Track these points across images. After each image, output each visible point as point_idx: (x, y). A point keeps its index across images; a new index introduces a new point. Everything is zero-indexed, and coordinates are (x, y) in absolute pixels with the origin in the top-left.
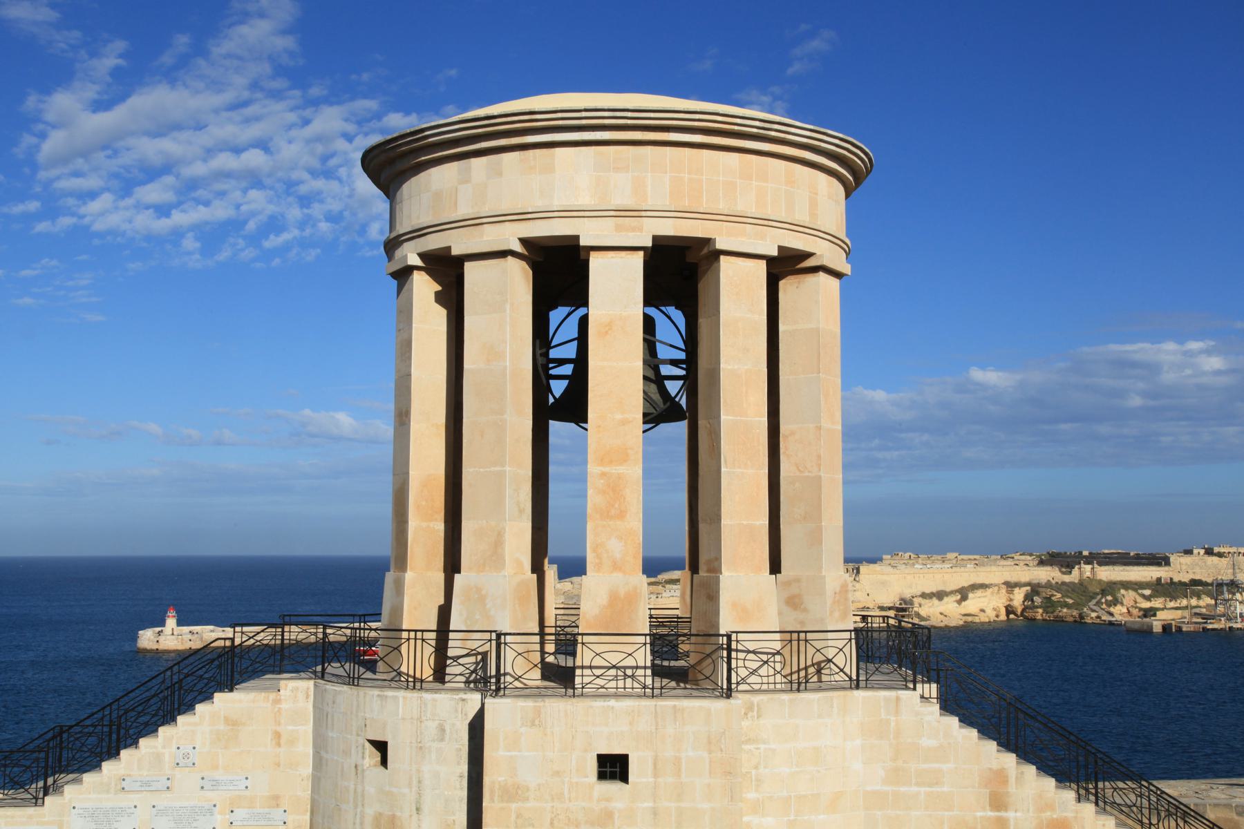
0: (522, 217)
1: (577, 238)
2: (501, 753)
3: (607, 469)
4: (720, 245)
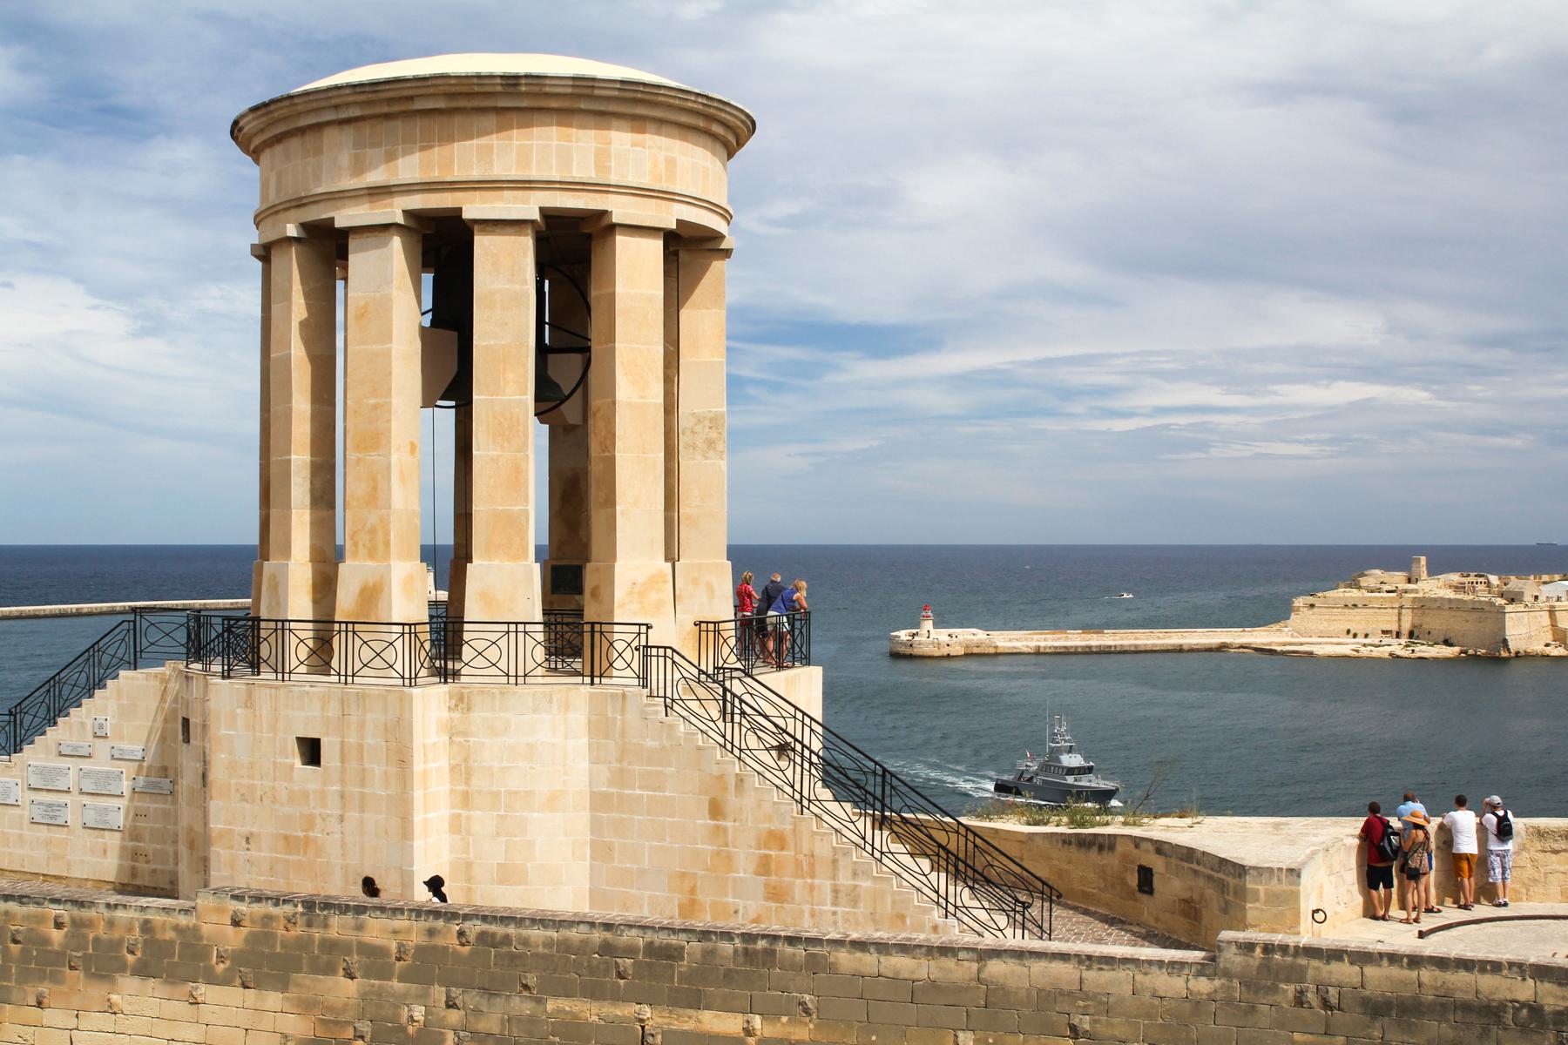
1: (332, 219)
4: (467, 214)
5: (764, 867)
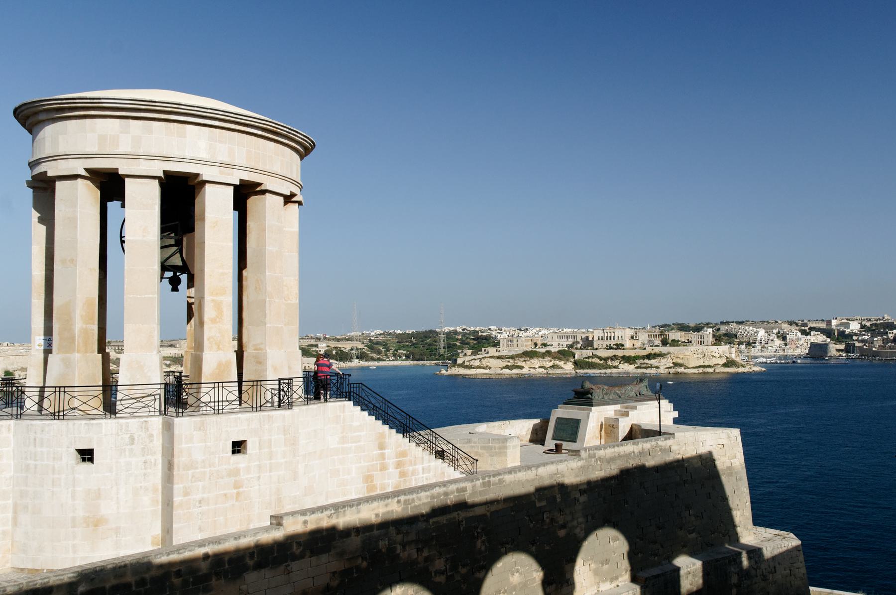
0: (166, 159)
2: (184, 446)
3: (215, 298)
5: (399, 465)
